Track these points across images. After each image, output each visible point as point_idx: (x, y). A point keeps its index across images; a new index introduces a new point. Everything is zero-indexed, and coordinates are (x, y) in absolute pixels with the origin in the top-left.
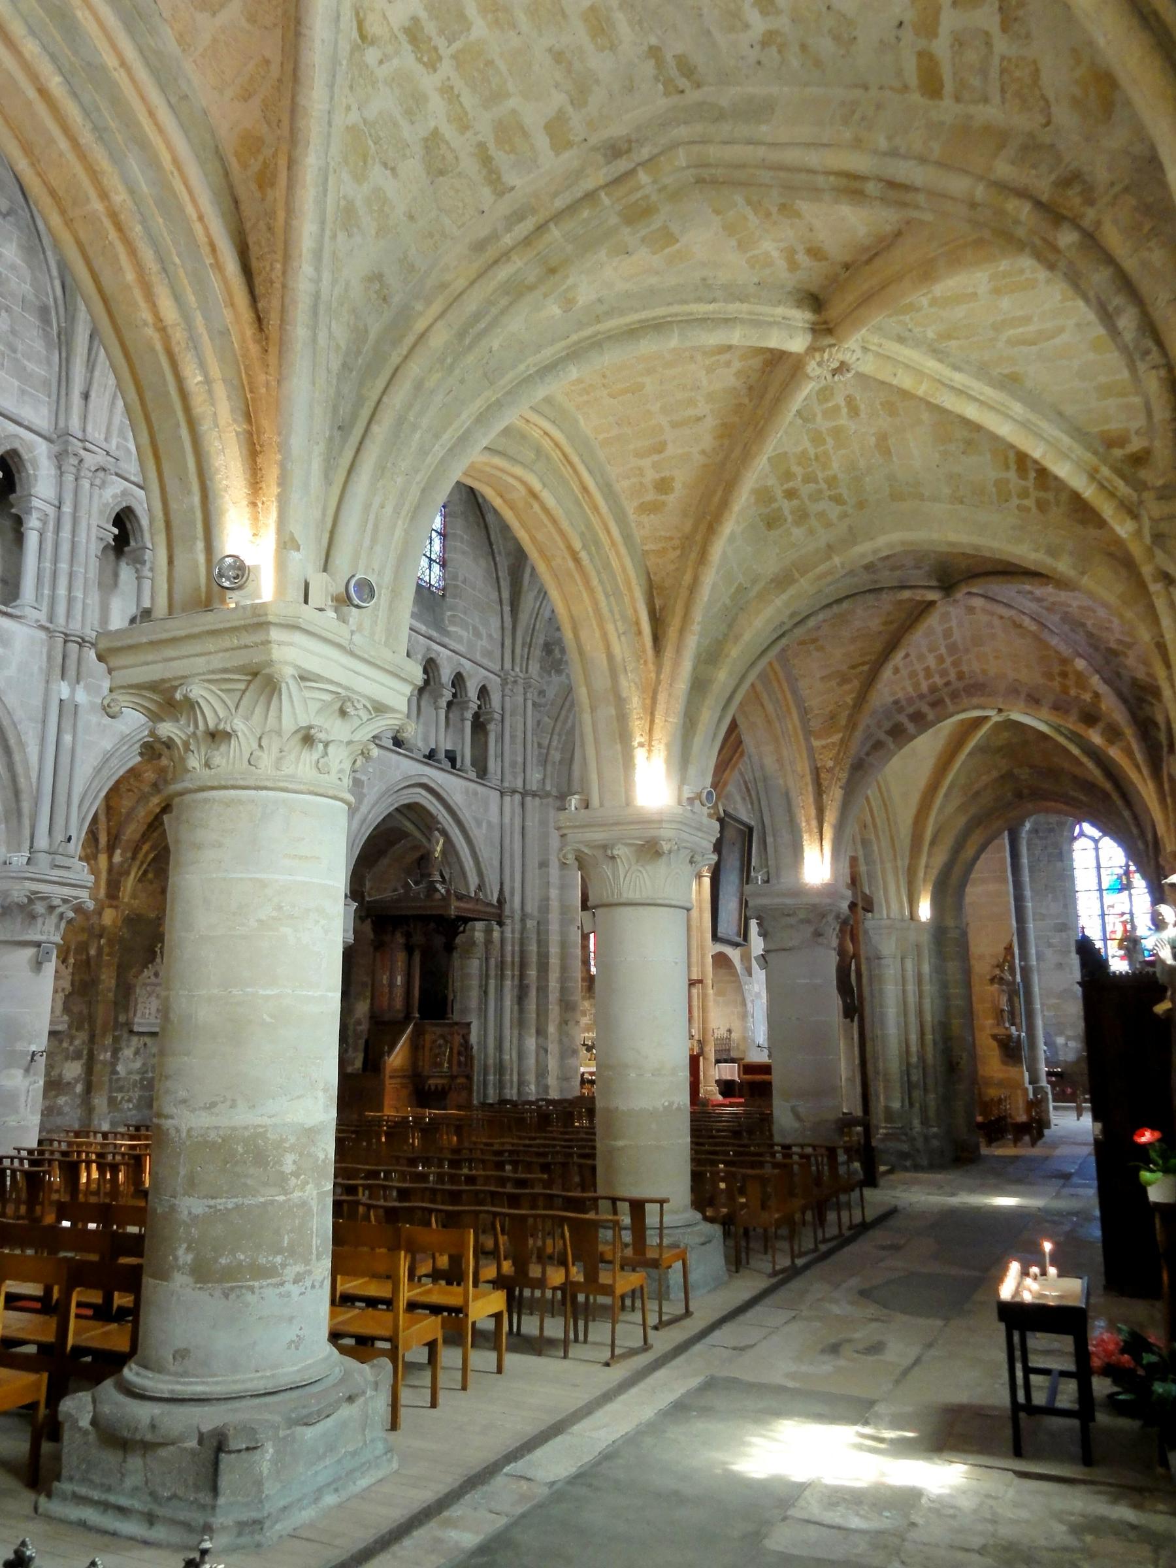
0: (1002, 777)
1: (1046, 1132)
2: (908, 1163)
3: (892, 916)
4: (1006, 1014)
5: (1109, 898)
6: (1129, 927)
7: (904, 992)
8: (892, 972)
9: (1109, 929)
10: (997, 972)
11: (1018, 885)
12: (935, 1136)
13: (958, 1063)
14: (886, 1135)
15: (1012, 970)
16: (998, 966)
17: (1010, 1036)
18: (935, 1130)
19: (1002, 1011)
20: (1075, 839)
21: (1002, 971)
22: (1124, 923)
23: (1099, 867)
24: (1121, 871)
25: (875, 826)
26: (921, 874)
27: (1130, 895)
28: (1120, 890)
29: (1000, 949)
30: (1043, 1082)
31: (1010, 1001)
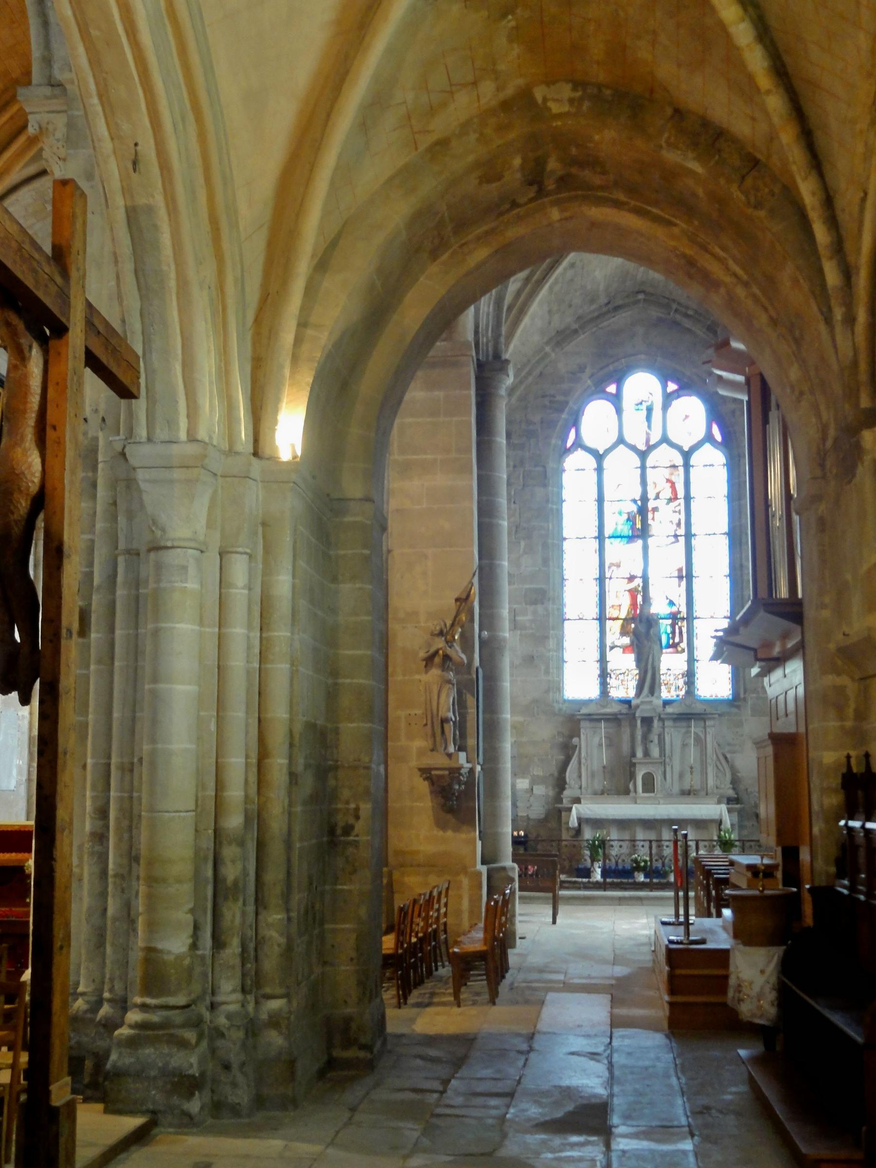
0: (505, 106)
1: (513, 957)
2: (194, 1106)
3: (202, 434)
4: (449, 728)
5: (614, 549)
6: (640, 599)
7: (221, 640)
8: (192, 585)
9: (610, 601)
10: (440, 643)
11: (486, 485)
12: (274, 1021)
13: (348, 830)
14: (142, 1026)
15: (466, 643)
16: (441, 633)
17: (455, 771)
18: (275, 1005)
19: (444, 721)
20: (568, 451)
21: (450, 643)
22: (633, 593)
23: (600, 500)
24: (634, 508)
25: (165, 167)
26: (288, 337)
27: (645, 548)
28: (631, 539)
29: (449, 602)
30: (508, 862)
31: (460, 704)
